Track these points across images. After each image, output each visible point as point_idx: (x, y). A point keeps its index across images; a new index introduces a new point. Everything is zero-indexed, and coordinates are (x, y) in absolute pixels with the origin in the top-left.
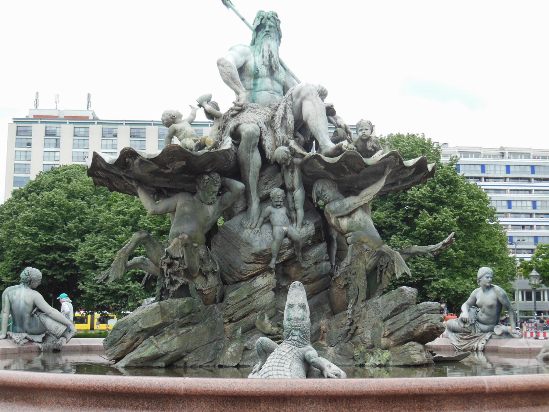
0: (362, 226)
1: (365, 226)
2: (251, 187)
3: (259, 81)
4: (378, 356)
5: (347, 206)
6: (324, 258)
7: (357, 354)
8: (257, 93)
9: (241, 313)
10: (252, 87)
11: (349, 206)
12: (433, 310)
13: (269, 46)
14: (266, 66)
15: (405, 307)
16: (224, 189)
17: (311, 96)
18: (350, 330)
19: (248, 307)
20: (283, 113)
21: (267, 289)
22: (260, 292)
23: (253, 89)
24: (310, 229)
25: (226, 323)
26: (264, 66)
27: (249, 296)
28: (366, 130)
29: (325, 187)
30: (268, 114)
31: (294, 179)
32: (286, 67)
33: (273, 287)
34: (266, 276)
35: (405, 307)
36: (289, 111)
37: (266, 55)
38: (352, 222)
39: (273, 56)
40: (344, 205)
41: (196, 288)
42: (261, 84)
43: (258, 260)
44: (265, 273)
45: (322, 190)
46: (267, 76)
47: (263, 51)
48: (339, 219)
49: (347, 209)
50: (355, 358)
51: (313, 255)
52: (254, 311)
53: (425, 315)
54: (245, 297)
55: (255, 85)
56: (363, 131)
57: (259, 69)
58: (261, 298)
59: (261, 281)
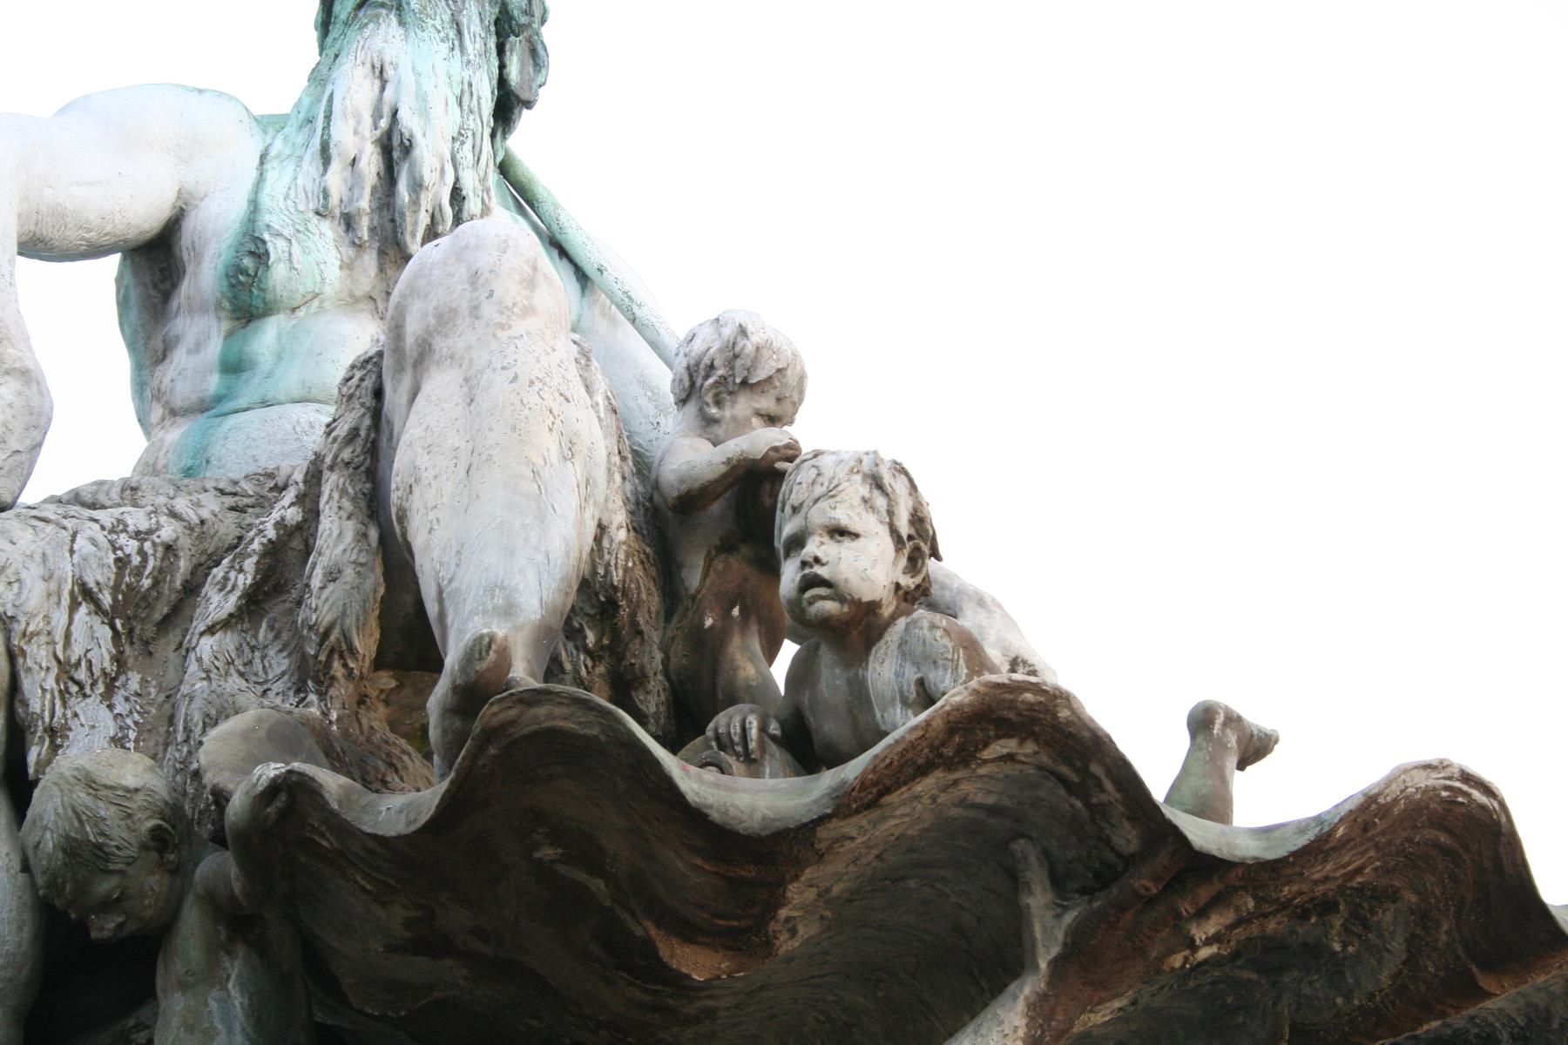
3: (267, 336)
8: (232, 420)
10: (214, 383)
13: (381, 74)
14: (349, 222)
17: (463, 323)
20: (294, 515)
23: (219, 399)
26: (328, 231)
28: (839, 532)
30: (168, 531)
32: (577, 260)
36: (331, 482)
37: (356, 138)
39: (407, 149)
42: (279, 357)
46: (352, 302)
47: (328, 117)
55: (234, 366)
56: (812, 548)
57: (276, 248)
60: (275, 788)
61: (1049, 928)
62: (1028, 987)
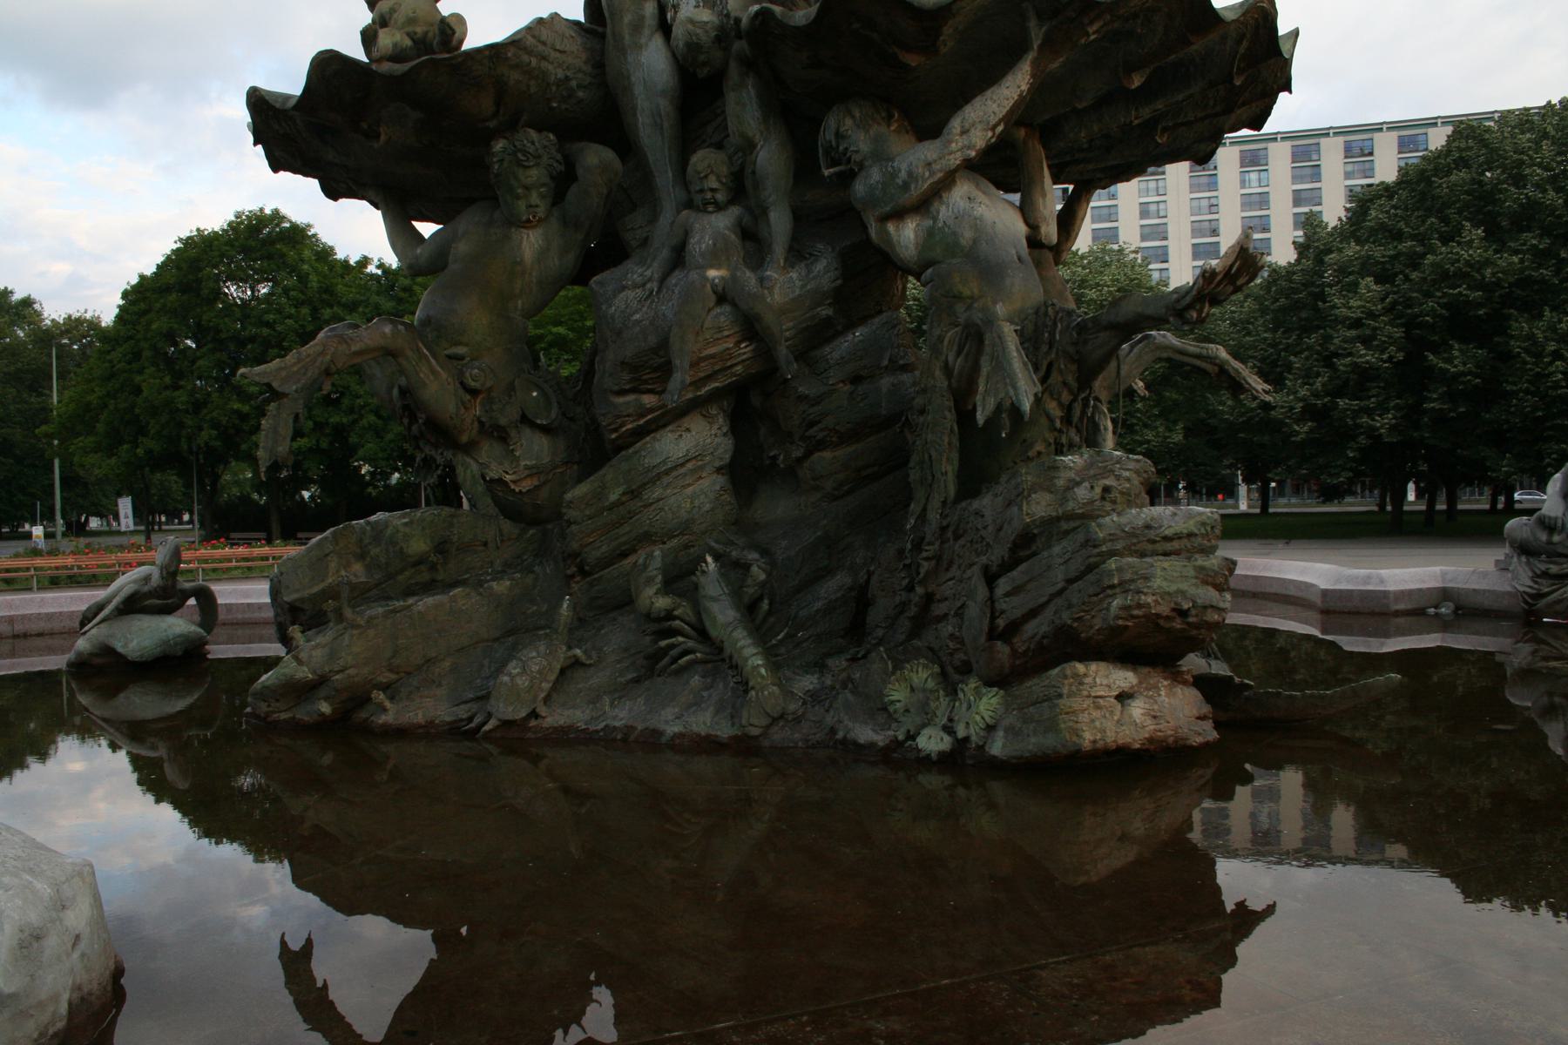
0: (963, 242)
1: (975, 241)
2: (651, 159)
4: (965, 706)
5: (903, 174)
6: (886, 362)
7: (896, 696)
9: (604, 549)
11: (910, 174)
12: (1166, 539)
15: (1065, 526)
16: (564, 179)
18: (904, 606)
19: (626, 528)
21: (693, 471)
22: (666, 480)
24: (824, 269)
25: (573, 576)
27: (634, 494)
29: (849, 122)
31: (743, 108)
33: (717, 464)
34: (688, 430)
35: (1065, 526)
38: (930, 233)
40: (894, 175)
41: (483, 477)
43: (646, 382)
44: (686, 422)
45: (838, 135)
48: (891, 227)
49: (906, 186)
50: (891, 709)
51: (836, 355)
52: (647, 538)
53: (1112, 564)
54: (613, 497)
58: (673, 499)
59: (672, 445)
60: (757, 14)
61: (1037, 34)
62: (1031, 56)
